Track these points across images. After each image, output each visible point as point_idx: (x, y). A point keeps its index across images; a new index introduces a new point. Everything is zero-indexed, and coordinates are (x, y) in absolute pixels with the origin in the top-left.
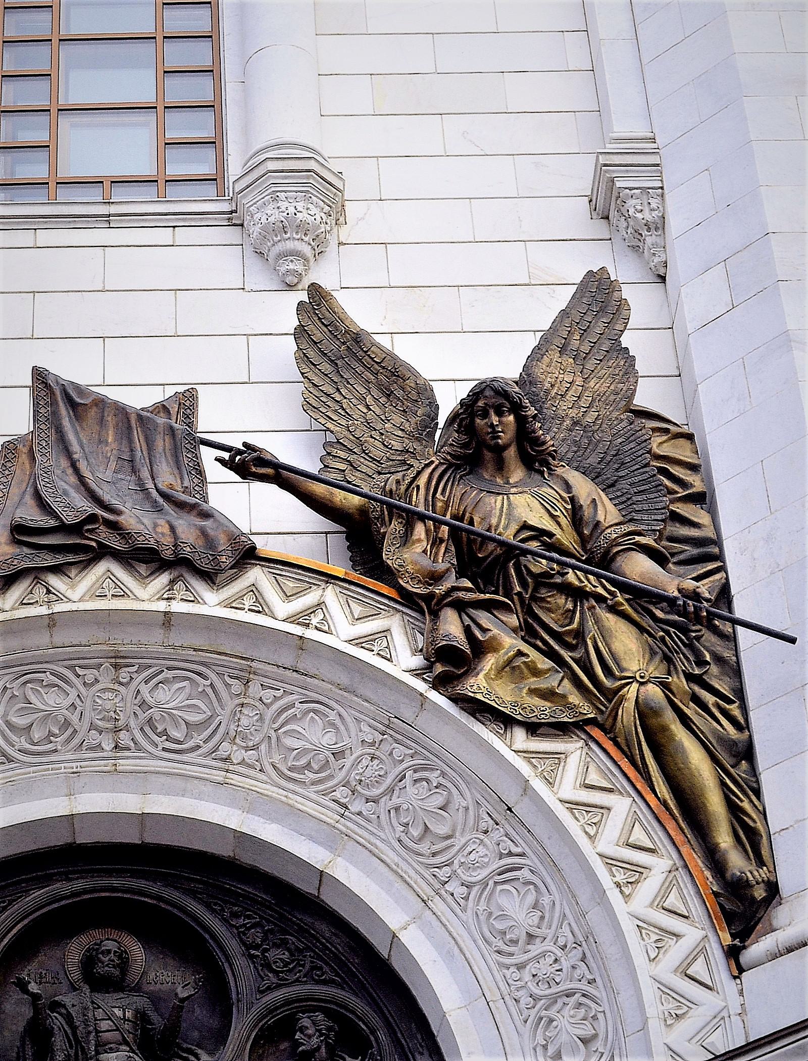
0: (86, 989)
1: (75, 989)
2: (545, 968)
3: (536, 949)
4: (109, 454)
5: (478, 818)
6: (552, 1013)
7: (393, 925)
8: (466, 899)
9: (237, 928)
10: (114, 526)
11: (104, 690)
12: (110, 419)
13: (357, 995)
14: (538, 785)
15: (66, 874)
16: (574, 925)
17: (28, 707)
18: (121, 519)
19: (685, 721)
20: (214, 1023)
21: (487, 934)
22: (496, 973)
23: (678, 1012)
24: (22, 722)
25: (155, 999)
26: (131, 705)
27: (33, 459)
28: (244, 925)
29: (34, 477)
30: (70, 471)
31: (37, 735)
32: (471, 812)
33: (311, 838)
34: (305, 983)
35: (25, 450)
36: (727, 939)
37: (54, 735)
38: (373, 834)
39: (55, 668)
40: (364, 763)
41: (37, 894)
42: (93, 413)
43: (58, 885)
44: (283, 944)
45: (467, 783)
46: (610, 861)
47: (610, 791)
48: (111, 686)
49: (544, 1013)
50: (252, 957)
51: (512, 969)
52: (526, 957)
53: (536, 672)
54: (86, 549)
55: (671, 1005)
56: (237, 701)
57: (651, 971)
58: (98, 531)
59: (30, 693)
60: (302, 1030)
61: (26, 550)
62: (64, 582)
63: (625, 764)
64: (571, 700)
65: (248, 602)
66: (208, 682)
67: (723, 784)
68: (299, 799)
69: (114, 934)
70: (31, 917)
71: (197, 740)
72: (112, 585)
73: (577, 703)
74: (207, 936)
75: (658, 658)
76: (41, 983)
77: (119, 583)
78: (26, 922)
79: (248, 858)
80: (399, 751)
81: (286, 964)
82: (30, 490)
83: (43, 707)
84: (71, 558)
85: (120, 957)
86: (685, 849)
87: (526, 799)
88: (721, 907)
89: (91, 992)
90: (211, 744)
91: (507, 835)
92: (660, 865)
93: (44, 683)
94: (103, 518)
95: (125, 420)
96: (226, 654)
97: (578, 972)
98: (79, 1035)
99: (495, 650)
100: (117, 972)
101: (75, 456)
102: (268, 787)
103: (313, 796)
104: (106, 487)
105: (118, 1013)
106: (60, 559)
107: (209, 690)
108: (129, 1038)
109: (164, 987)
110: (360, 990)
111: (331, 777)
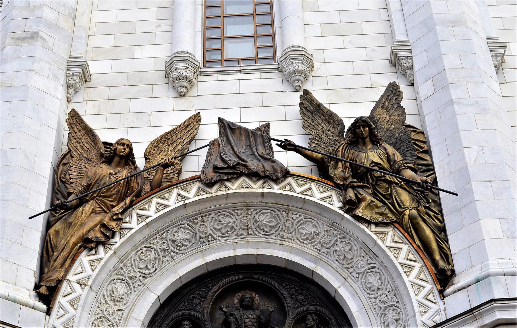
0: (241, 309)
2: (383, 298)
3: (380, 293)
5: (361, 253)
6: (386, 312)
8: (358, 278)
10: (245, 166)
11: (244, 217)
14: (379, 242)
15: (233, 274)
17: (220, 223)
18: (247, 164)
19: (424, 221)
21: (365, 288)
26: (252, 221)
27: (219, 146)
29: (220, 152)
30: (231, 149)
31: (223, 231)
32: (359, 251)
33: (309, 261)
36: (439, 288)
37: (229, 231)
40: (325, 237)
42: (238, 131)
44: (302, 293)
45: (357, 242)
52: (377, 295)
53: (378, 207)
55: (422, 309)
57: (416, 298)
60: (308, 320)
61: (218, 174)
63: (406, 234)
65: (288, 188)
67: (436, 240)
71: (273, 231)
75: (415, 202)
79: (290, 267)
80: (336, 233)
84: (232, 176)
85: (251, 299)
86: (425, 260)
87: (376, 246)
90: (277, 233)
92: (418, 265)
100: (250, 304)
103: (310, 248)
104: (242, 154)
105: (251, 316)
106: (229, 177)
107: (276, 216)
108: (255, 324)
109: (266, 308)
111: (315, 241)
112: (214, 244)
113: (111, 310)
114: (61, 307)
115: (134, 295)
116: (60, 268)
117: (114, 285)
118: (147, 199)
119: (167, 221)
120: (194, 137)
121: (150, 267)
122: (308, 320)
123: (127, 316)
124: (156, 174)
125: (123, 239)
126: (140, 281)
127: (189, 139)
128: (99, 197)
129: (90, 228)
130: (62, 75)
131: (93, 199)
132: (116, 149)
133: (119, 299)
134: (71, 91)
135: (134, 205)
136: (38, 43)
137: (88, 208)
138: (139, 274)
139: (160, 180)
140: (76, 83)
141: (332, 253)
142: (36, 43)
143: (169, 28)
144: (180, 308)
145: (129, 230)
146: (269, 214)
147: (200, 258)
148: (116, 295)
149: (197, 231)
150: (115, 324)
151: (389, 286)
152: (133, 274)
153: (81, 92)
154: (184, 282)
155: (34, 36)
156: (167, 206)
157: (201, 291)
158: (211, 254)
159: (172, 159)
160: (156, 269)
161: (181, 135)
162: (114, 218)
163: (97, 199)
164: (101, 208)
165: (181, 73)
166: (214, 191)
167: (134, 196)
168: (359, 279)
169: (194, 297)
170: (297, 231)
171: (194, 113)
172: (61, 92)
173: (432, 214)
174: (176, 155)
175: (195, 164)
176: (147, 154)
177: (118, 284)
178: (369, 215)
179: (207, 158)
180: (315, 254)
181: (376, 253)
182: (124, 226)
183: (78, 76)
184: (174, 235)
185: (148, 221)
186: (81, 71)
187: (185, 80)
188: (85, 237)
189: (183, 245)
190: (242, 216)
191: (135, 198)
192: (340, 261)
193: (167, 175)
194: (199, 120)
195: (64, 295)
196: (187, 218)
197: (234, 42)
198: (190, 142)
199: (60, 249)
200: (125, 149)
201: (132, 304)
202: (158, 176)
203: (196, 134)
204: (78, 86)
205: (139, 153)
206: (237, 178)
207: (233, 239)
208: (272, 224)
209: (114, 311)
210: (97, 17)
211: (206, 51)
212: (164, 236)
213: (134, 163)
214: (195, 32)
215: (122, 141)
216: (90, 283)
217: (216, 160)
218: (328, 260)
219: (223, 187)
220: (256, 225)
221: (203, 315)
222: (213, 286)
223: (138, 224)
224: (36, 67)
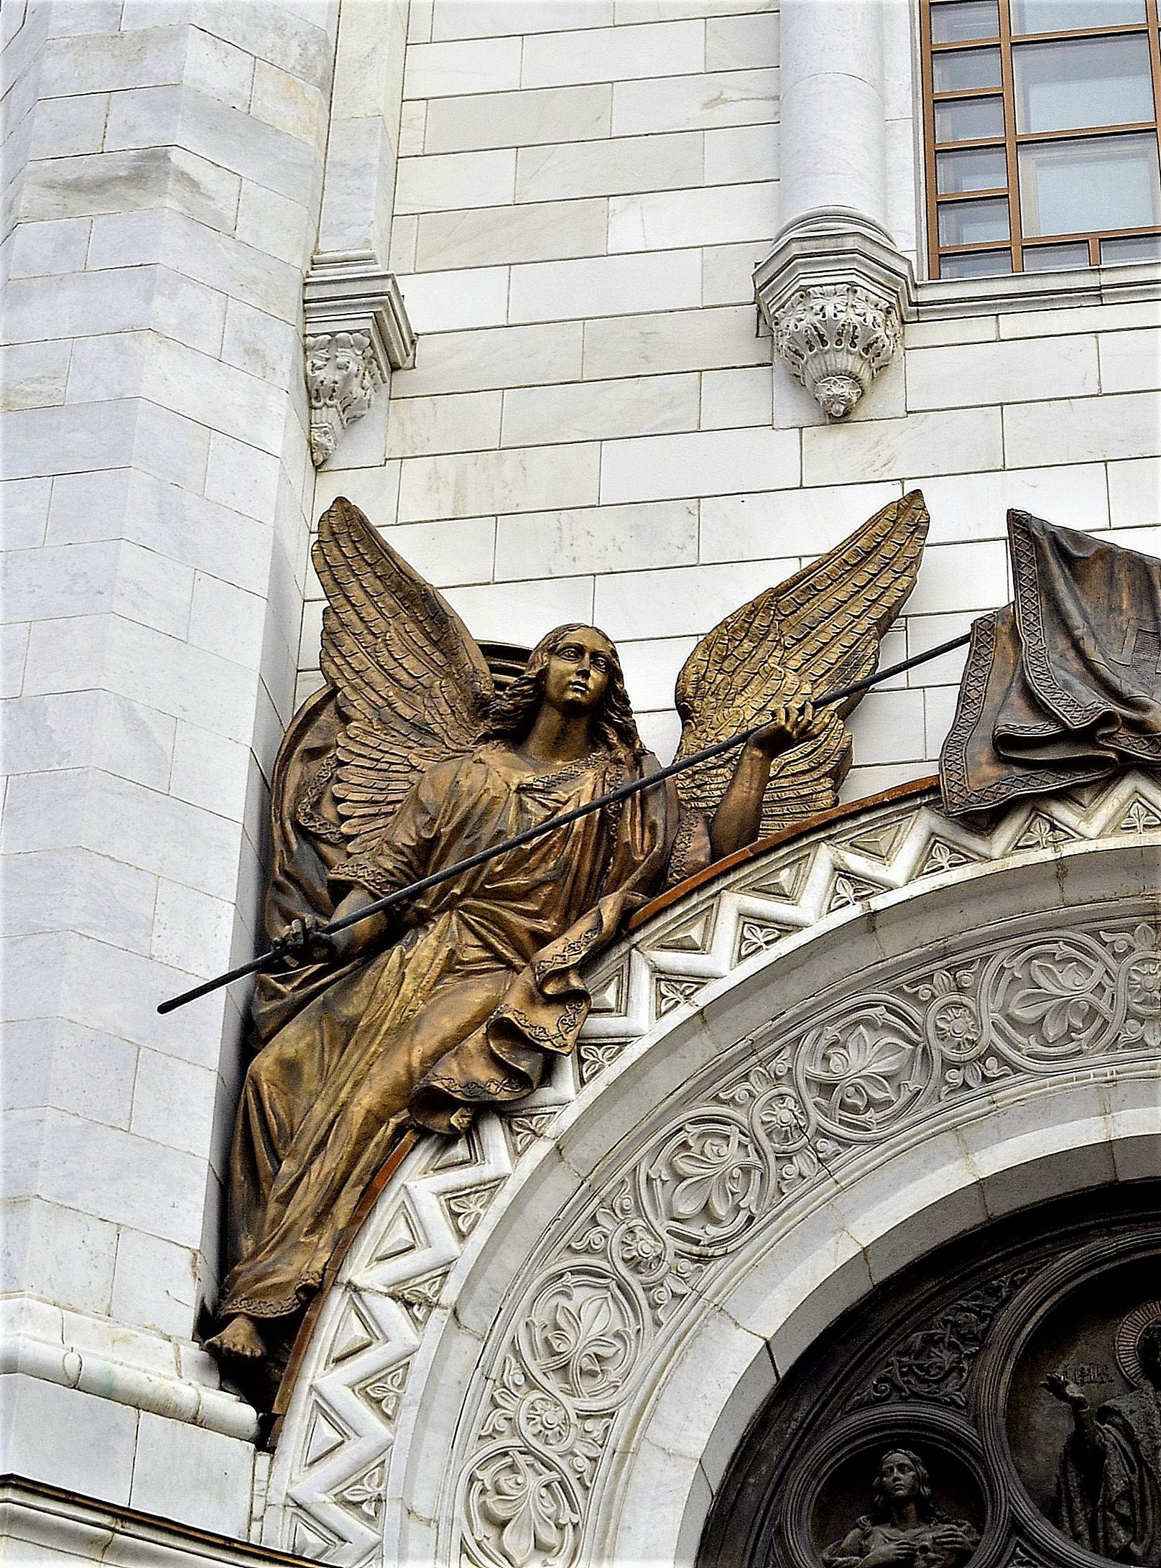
0: (1148, 1386)
1: (1133, 1389)
4: (1125, 626)
10: (1139, 728)
11: (1142, 961)
12: (1123, 576)
15: (1107, 1226)
18: (1148, 716)
27: (1017, 641)
29: (1020, 667)
30: (1071, 654)
31: (1051, 1032)
35: (1005, 629)
37: (1078, 1031)
39: (1071, 934)
41: (1069, 1258)
42: (1098, 569)
43: (1097, 1242)
54: (1101, 763)
58: (1117, 736)
59: (1038, 972)
61: (1017, 771)
62: (1074, 813)
70: (1063, 1291)
72: (1143, 812)
76: (1083, 1383)
77: (1152, 808)
78: (1055, 1298)
82: (1016, 685)
83: (1058, 992)
84: (1081, 778)
89: (1156, 1390)
93: (1057, 958)
94: (1123, 717)
95: (1144, 577)
98: (1143, 1452)
101: (1076, 632)
104: (1123, 673)
106: (1065, 781)
112: (1010, 1090)
113: (552, 1416)
114: (324, 1409)
115: (653, 1343)
116: (311, 1231)
117: (563, 1301)
118: (695, 899)
120: (900, 603)
121: (720, 1209)
123: (629, 1440)
124: (732, 784)
125: (595, 1088)
126: (679, 1275)
127: (876, 613)
128: (475, 897)
129: (443, 1042)
130: (281, 344)
131: (450, 907)
132: (544, 674)
133: (586, 1364)
134: (328, 416)
135: (638, 929)
136: (169, 203)
137: (426, 949)
139: (751, 806)
140: (347, 380)
142: (157, 201)
143: (764, 110)
144: (869, 1393)
147: (952, 1159)
148: (575, 1346)
149: (931, 1034)
150: (573, 1478)
152: (646, 1246)
153: (374, 421)
155: (149, 169)
156: (788, 928)
157: (963, 1309)
158: (1000, 1140)
159: (801, 711)
160: (751, 1219)
161: (841, 596)
162: (550, 990)
163: (467, 909)
164: (487, 946)
165: (830, 311)
166: (1002, 850)
167: (635, 888)
169: (930, 1341)
171: (894, 493)
172: (278, 424)
174: (823, 690)
175: (908, 730)
176: (690, 691)
177: (579, 1295)
179: (963, 699)
182: (598, 1024)
183: (357, 345)
184: (826, 1058)
185: (704, 997)
186: (369, 324)
187: (846, 344)
188: (422, 1083)
189: (870, 1104)
190: (1136, 956)
191: (639, 898)
193: (784, 782)
194: (921, 528)
195: (336, 1354)
196: (885, 977)
197: (1062, 162)
198: (884, 626)
199: (306, 1143)
200: (586, 674)
201: (647, 1383)
202: (743, 791)
203: (907, 592)
204: (358, 392)
205: (649, 687)
206: (1104, 786)
207: (1098, 1065)
210: (434, 71)
211: (939, 204)
212: (779, 1066)
213: (628, 735)
214: (886, 123)
215: (573, 639)
216: (449, 1295)
217: (1003, 705)
219: (1041, 830)
221: (976, 1422)
222: (1015, 1286)
223: (660, 1015)
224: (164, 311)
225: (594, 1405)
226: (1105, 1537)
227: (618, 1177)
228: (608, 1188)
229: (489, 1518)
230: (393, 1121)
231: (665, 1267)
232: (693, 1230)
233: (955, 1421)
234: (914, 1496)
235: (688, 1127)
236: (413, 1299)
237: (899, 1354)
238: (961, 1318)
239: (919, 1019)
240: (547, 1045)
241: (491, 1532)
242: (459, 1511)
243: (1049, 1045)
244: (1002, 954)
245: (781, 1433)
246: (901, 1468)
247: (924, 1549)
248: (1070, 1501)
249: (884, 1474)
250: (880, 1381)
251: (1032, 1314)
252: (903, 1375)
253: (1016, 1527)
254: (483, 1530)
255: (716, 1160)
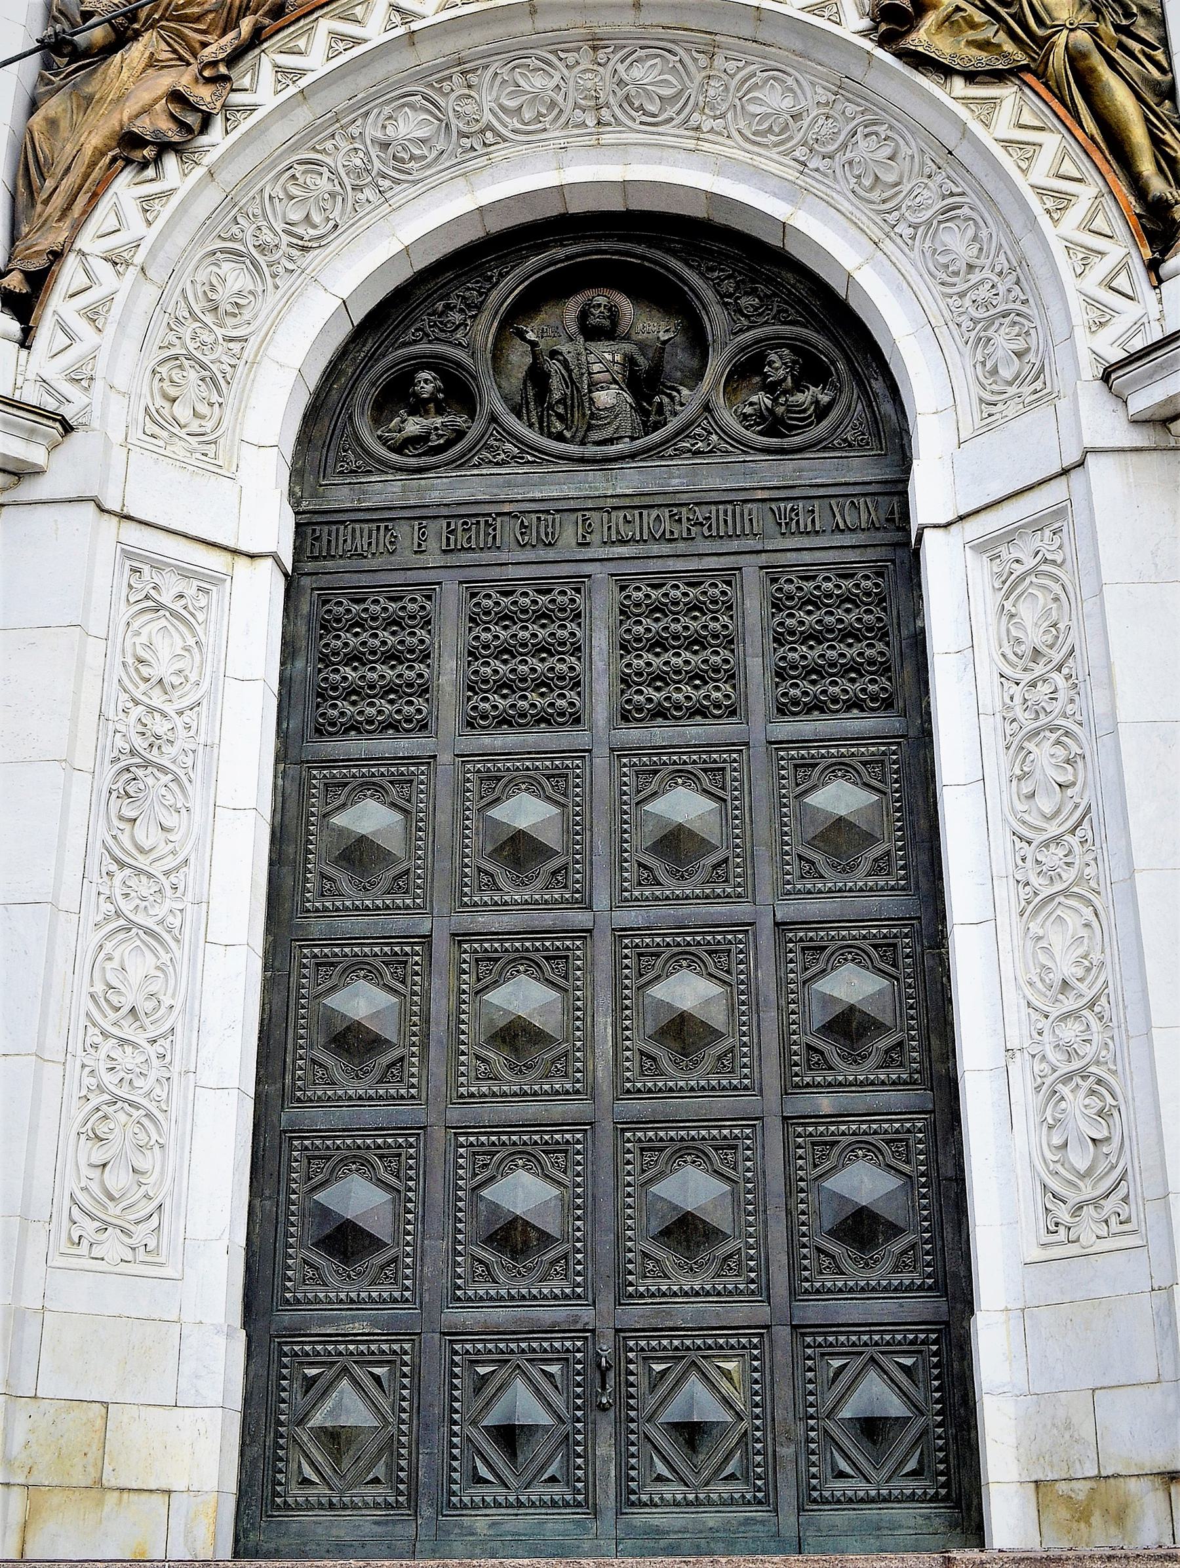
0: (581, 339)
1: (572, 340)
2: (983, 293)
3: (975, 278)
5: (922, 164)
7: (849, 266)
8: (913, 238)
9: (713, 280)
11: (585, 71)
13: (818, 332)
14: (975, 127)
16: (1009, 252)
17: (518, 90)
19: (1112, 63)
20: (695, 363)
21: (933, 269)
22: (940, 302)
23: (1102, 320)
24: (512, 104)
25: (642, 346)
26: (610, 84)
28: (718, 277)
31: (527, 115)
32: (916, 160)
33: (775, 195)
34: (773, 324)
36: (1148, 254)
37: (544, 116)
38: (829, 187)
39: (539, 52)
40: (820, 122)
44: (753, 292)
45: (912, 133)
46: (1041, 191)
47: (1042, 129)
48: (591, 67)
49: (982, 334)
50: (726, 304)
51: (955, 297)
52: (967, 285)
53: (973, 26)
55: (1094, 314)
56: (704, 74)
57: (1078, 286)
60: (770, 364)
63: (1055, 104)
64: (1005, 49)
66: (677, 58)
67: (1147, 120)
68: (763, 160)
69: (606, 292)
71: (670, 112)
73: (1011, 51)
74: (686, 289)
75: (1086, 9)
78: (526, 283)
79: (720, 218)
80: (851, 109)
81: (756, 309)
85: (610, 310)
86: (1110, 177)
87: (965, 142)
88: (1143, 226)
90: (683, 116)
91: (948, 177)
92: (1087, 193)
96: (692, 30)
97: (1013, 294)
99: (935, 7)
100: (607, 323)
102: (734, 151)
103: (776, 157)
105: (609, 357)
107: (678, 65)
108: (619, 378)
109: (650, 336)
110: (822, 329)
111: (791, 138)
112: (500, 152)
113: (206, 337)
115: (272, 298)
116: (59, 220)
117: (215, 269)
118: (302, 23)
119: (362, 83)
121: (317, 218)
122: (770, 364)
123: (256, 356)
125: (235, 136)
126: (290, 258)
128: (167, 20)
129: (142, 107)
131: (152, 27)
133: (229, 308)
135: (266, 40)
137: (136, 52)
138: (286, 239)
141: (839, 171)
144: (409, 337)
145: (252, 109)
146: (656, 61)
148: (223, 296)
149: (451, 114)
150: (220, 376)
151: (1002, 257)
152: (267, 237)
154: (422, 262)
156: (357, 41)
157: (469, 289)
158: (493, 183)
160: (336, 226)
162: (206, 74)
163: (162, 27)
164: (175, 51)
167: (265, 15)
168: (917, 243)
170: (739, 108)
173: (1136, 47)
177: (226, 266)
178: (948, 51)
180: (791, 175)
181: (967, 161)
182: (236, 98)
184: (384, 127)
185: (303, 83)
188: (126, 129)
189: (412, 158)
191: (267, 21)
192: (863, 194)
195: (70, 293)
196: (421, 76)
199: (60, 170)
201: (269, 322)
208: (666, 92)
209: (216, 341)
212: (354, 130)
216: (139, 258)
218: (829, 191)
220: (621, 93)
221: (473, 356)
222: (502, 276)
223: (277, 93)
225: (235, 333)
226: (548, 426)
227: (251, 195)
228: (244, 201)
229: (165, 396)
230: (111, 154)
231: (281, 252)
232: (300, 230)
233: (461, 355)
234: (433, 398)
235: (296, 166)
236: (117, 260)
237: (429, 315)
238: (467, 294)
239: (443, 104)
240: (204, 108)
241: (167, 405)
242: (146, 390)
243: (526, 124)
244: (496, 64)
245: (355, 358)
246: (426, 383)
247: (436, 429)
248: (528, 403)
249: (415, 385)
250: (417, 330)
251: (511, 293)
252: (430, 327)
253: (493, 419)
254: (160, 402)
255: (313, 187)
